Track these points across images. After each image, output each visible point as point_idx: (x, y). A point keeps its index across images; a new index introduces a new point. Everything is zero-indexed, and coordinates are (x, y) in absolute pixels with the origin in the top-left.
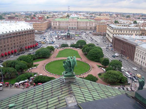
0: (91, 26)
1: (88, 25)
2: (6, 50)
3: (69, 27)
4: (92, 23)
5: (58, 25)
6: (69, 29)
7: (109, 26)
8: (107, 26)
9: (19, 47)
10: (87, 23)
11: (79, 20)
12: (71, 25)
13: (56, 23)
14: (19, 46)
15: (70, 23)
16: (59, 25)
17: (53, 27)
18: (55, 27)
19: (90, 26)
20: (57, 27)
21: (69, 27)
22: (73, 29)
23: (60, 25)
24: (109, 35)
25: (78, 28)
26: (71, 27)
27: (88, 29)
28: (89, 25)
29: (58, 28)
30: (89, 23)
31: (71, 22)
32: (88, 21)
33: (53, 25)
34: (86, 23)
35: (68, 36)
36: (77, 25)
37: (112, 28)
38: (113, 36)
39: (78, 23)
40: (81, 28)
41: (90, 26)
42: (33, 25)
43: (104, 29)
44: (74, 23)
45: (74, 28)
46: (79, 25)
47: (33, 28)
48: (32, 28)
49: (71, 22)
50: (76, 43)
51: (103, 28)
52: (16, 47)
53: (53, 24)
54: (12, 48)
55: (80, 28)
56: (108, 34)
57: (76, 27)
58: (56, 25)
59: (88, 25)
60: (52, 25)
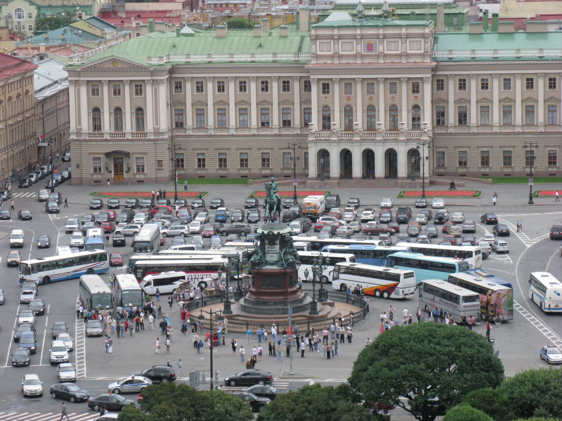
3: (324, 154)
5: (159, 119)
6: (313, 171)
11: (457, 46)
12: (348, 112)
15: (336, 89)
16: (180, 125)
17: (83, 160)
18: (118, 159)
20: (154, 161)
21: (324, 154)
22: (357, 170)
23: (190, 120)
25: (451, 163)
26: (346, 156)
31: (348, 85)
33: (97, 126)
35: (260, 278)
36: (427, 119)
39: (452, 86)
40: (496, 164)
44: (393, 85)
45: (391, 156)
46: (463, 118)
49: (348, 85)
50: (345, 381)
53: (96, 112)
55: (474, 164)
57: (413, 154)
60: (79, 121)
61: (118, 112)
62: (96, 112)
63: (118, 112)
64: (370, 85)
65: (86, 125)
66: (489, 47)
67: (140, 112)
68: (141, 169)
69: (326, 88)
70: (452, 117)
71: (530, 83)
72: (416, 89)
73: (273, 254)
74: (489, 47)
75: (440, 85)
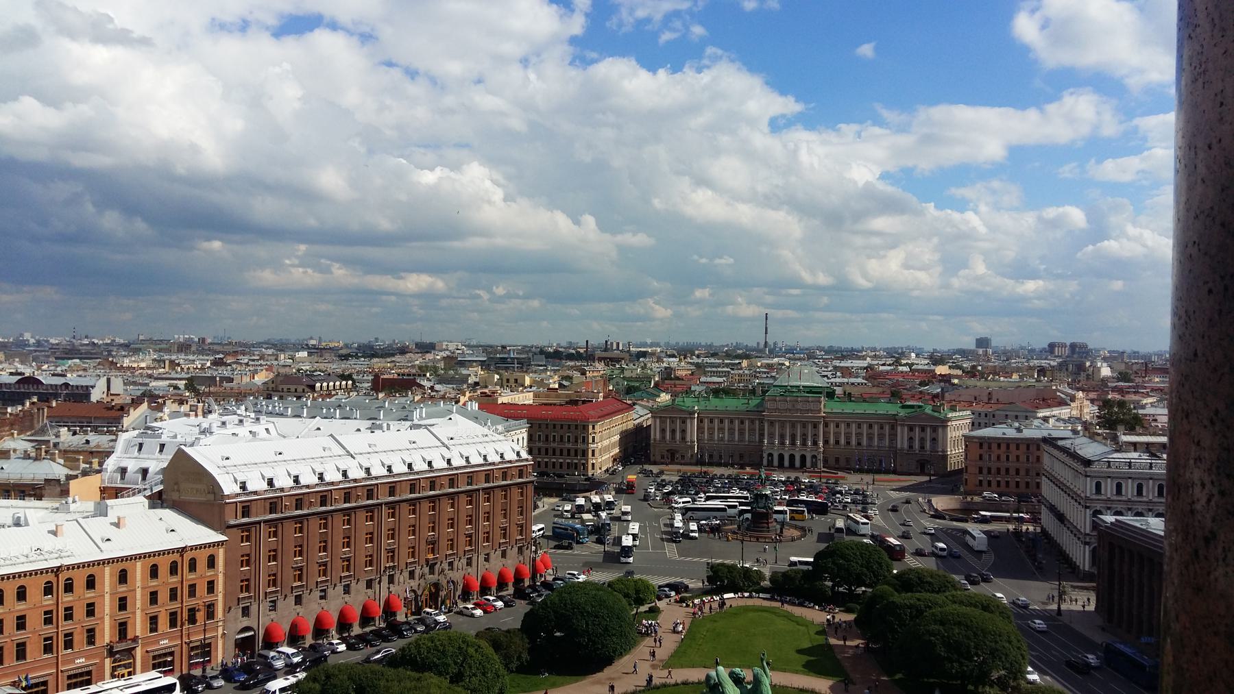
0: (922, 447)
1: (902, 442)
2: (330, 591)
3: (770, 455)
4: (935, 429)
6: (765, 462)
7: (1064, 450)
8: (1046, 447)
9: (422, 576)
10: (893, 427)
13: (684, 422)
14: (418, 572)
17: (655, 453)
19: (917, 445)
24: (1061, 517)
25: (832, 462)
27: (899, 469)
28: (911, 447)
29: (694, 461)
30: (911, 429)
32: (902, 413)
33: (663, 438)
34: (887, 428)
37: (1087, 463)
38: (1095, 526)
39: (832, 426)
41: (917, 445)
42: (525, 435)
43: (1022, 472)
46: (837, 442)
47: (524, 455)
48: (518, 454)
51: (1012, 465)
52: (401, 577)
54: (369, 584)
55: (842, 463)
56: (1052, 509)
57: (814, 457)
58: (683, 438)
59: (902, 442)
60: (655, 435)
61: (673, 432)
62: (663, 431)
63: (673, 432)
64: (793, 425)
65: (658, 437)
66: (849, 408)
67: (683, 431)
68: (683, 457)
69: (772, 423)
70: (832, 441)
71: (871, 426)
72: (815, 426)
73: (762, 503)
74: (849, 408)
75: (826, 425)
